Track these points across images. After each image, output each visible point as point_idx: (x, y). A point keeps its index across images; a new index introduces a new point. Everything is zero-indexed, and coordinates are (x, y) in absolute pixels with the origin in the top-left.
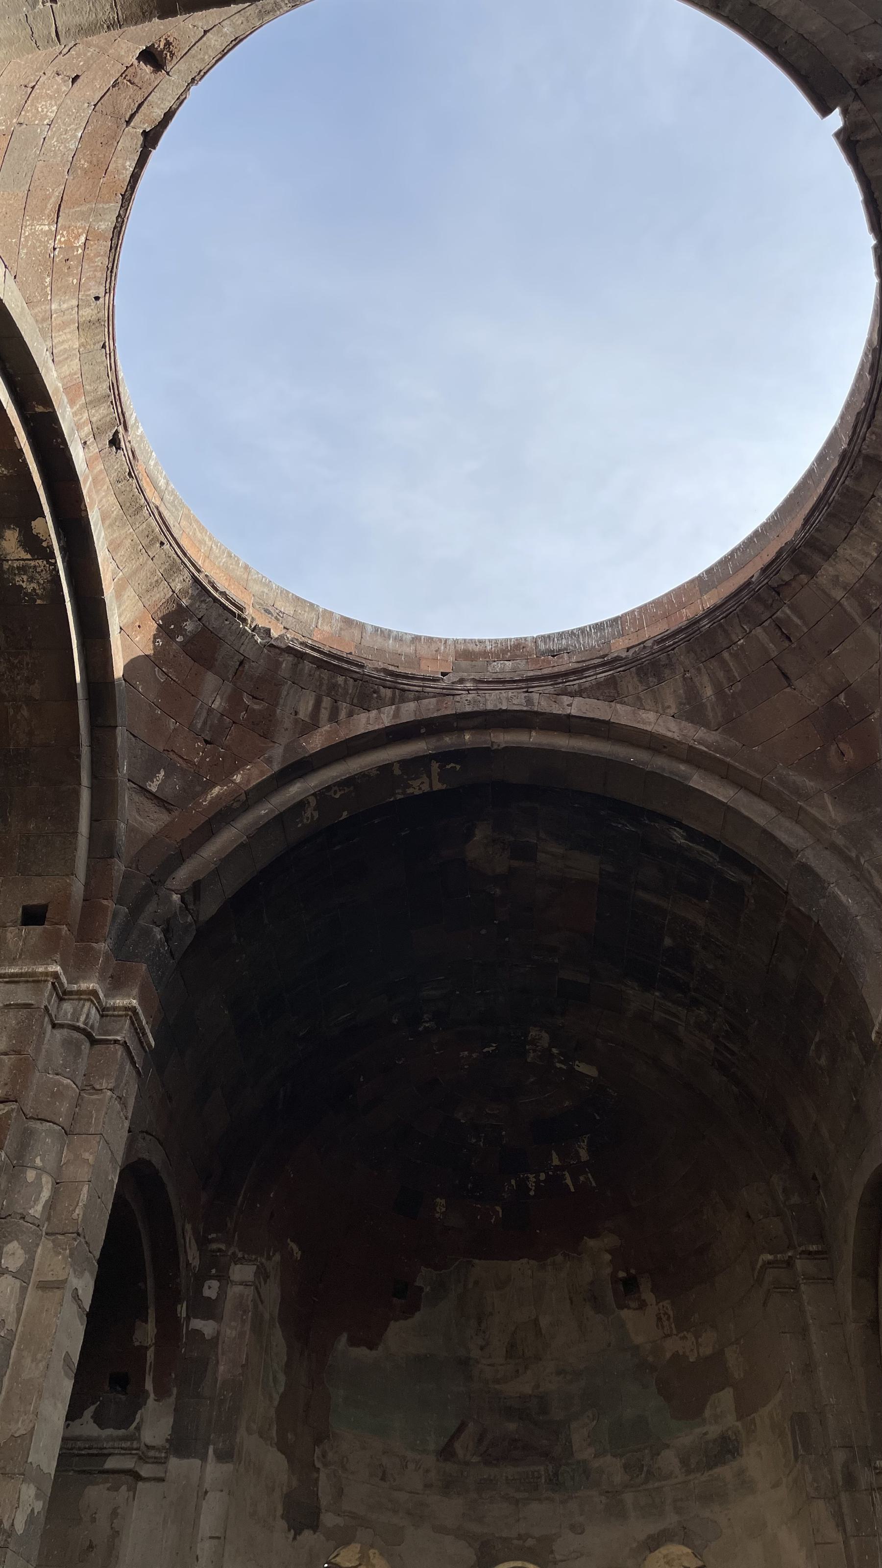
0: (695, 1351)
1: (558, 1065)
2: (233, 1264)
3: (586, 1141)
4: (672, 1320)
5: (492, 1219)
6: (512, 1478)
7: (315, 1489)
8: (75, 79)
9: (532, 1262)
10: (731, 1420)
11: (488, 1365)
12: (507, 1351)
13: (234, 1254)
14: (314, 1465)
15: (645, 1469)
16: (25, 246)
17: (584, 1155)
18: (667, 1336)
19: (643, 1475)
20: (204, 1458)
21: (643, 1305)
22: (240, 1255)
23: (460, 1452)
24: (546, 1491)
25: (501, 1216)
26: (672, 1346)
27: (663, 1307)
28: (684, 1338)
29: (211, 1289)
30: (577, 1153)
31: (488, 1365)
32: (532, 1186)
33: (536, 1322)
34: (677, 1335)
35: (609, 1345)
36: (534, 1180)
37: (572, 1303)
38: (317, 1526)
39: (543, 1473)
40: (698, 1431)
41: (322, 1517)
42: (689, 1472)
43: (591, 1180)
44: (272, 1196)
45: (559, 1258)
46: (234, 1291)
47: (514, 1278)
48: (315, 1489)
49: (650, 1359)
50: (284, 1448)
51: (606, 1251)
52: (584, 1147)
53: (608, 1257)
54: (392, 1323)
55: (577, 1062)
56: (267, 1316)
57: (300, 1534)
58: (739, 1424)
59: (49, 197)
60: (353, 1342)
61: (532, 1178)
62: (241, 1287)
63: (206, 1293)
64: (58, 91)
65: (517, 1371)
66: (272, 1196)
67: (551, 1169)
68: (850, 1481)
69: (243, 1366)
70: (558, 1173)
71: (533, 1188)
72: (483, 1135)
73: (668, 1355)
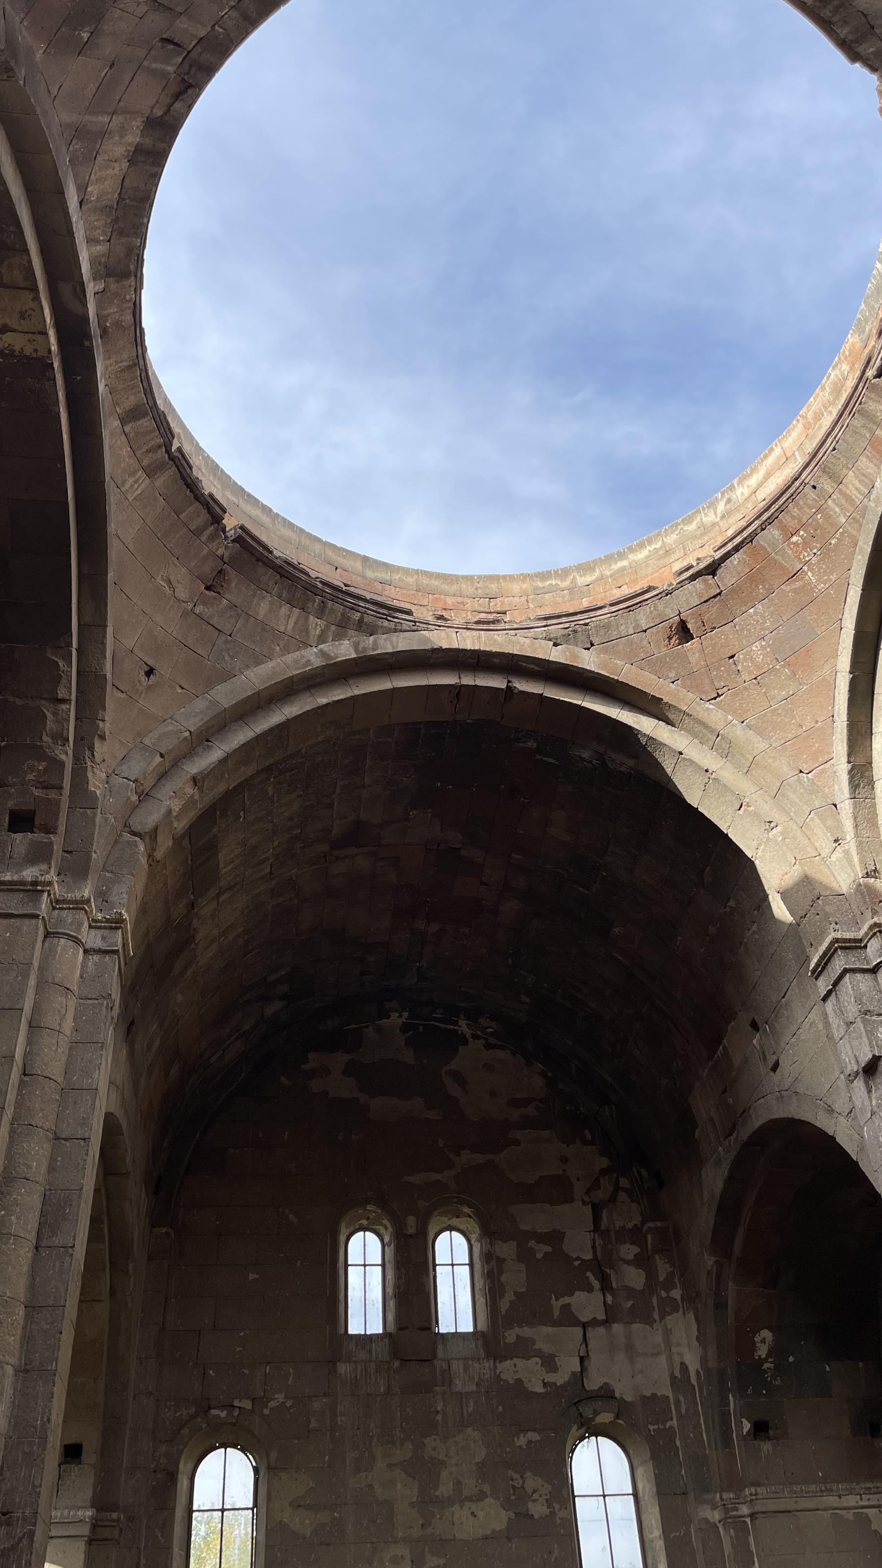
8: (733, 657)
16: (830, 580)
59: (795, 591)
64: (745, 660)
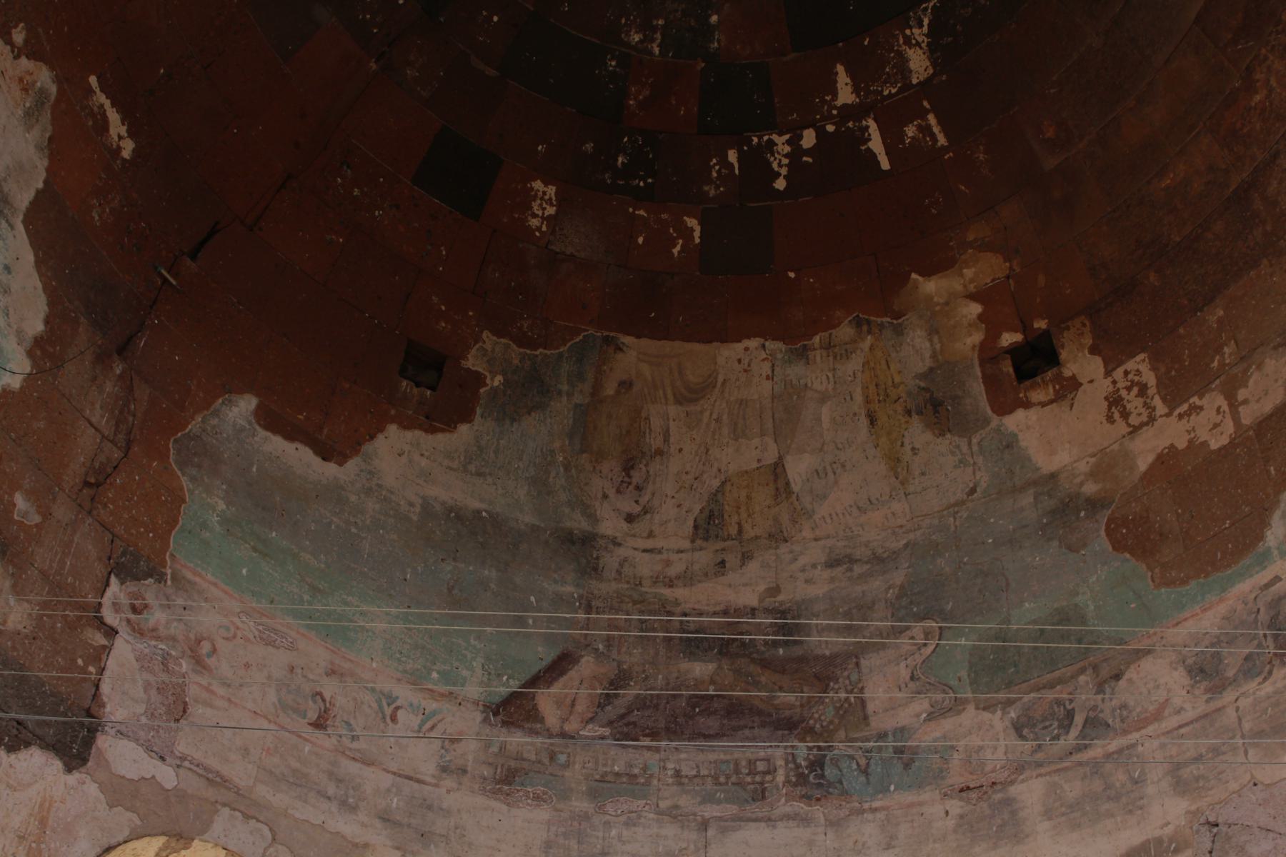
3: (926, 22)
5: (675, 246)
6: (694, 773)
9: (770, 345)
11: (645, 551)
12: (696, 527)
15: (1079, 719)
17: (919, 64)
18: (1135, 430)
21: (1070, 387)
23: (551, 715)
24: (786, 801)
25: (697, 240)
27: (1126, 373)
30: (903, 60)
31: (645, 551)
32: (780, 166)
33: (777, 469)
34: (1168, 415)
36: (787, 149)
37: (872, 420)
38: (84, 761)
39: (780, 763)
40: (1245, 587)
42: (1217, 689)
43: (936, 130)
45: (845, 331)
47: (725, 381)
48: (91, 669)
51: (973, 297)
52: (920, 40)
53: (975, 309)
54: (392, 429)
60: (270, 419)
61: (781, 141)
65: (722, 563)
67: (834, 116)
70: (850, 124)
71: (784, 171)
72: (661, 22)
73: (1143, 465)
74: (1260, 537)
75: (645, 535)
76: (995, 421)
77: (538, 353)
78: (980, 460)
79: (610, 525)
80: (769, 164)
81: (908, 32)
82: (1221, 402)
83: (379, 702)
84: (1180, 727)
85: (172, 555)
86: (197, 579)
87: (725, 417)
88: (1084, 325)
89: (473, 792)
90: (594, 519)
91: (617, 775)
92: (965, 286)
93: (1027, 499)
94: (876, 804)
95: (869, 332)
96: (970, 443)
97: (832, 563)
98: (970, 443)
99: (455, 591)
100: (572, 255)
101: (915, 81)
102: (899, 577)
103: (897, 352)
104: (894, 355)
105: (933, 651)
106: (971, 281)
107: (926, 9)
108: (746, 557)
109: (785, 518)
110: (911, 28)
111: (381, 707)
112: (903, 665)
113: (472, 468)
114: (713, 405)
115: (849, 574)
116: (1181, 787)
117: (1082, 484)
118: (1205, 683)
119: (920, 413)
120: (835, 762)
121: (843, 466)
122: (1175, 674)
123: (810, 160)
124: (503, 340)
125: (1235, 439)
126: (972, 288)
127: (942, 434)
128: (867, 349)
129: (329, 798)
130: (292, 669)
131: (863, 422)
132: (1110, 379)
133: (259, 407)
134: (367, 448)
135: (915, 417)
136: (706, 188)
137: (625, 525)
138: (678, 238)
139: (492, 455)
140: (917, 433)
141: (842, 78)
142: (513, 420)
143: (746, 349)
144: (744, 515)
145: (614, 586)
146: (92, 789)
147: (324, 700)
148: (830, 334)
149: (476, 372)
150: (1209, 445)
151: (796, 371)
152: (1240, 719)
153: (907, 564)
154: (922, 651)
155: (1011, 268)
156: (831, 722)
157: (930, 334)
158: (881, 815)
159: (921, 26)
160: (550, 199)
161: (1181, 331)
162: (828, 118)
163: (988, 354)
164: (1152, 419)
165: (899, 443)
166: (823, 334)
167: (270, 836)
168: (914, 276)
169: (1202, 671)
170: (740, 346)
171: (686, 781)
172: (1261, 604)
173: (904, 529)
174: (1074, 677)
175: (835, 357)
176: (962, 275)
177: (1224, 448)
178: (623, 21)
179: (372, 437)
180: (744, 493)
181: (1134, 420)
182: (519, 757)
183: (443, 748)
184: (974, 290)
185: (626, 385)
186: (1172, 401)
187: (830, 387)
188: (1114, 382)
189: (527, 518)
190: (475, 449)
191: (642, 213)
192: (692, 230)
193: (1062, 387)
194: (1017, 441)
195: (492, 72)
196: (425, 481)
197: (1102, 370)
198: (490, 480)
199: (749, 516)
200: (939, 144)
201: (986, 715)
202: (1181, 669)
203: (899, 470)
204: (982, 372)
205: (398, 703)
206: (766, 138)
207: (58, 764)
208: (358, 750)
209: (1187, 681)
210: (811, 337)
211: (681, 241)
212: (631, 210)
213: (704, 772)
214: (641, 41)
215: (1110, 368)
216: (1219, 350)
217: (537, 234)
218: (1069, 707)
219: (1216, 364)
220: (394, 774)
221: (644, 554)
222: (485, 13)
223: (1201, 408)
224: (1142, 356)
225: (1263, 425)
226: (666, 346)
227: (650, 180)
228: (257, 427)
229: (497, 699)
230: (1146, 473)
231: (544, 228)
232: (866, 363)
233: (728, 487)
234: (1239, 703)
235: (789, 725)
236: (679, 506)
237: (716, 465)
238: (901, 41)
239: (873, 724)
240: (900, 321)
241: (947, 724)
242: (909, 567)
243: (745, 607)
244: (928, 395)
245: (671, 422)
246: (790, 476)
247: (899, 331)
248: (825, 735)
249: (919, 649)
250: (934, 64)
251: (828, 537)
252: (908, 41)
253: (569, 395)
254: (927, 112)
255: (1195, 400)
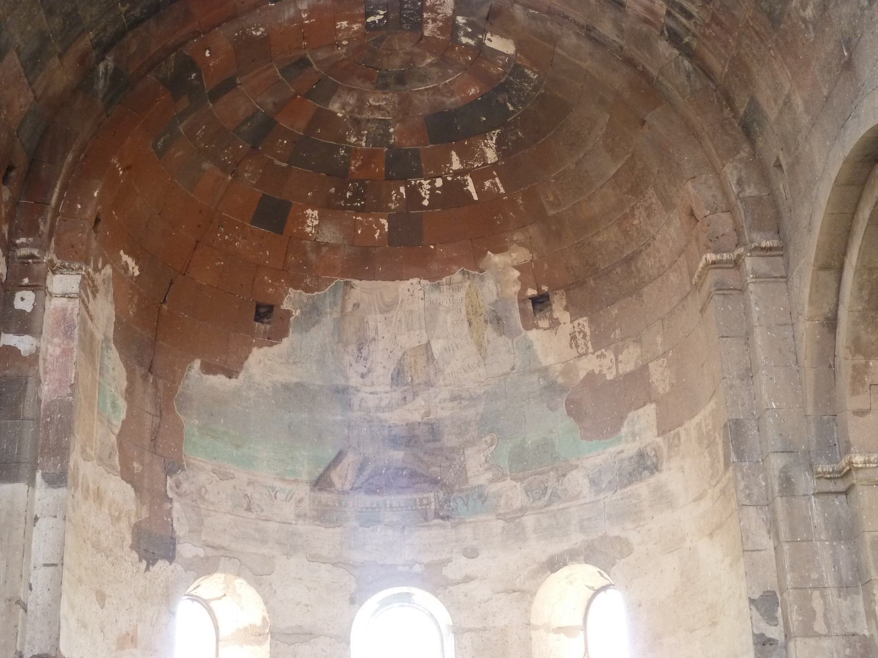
0: (614, 368)
1: (464, 40)
2: (50, 273)
4: (588, 338)
7: (169, 520)
9: (423, 282)
10: (650, 437)
12: (392, 379)
13: (51, 261)
14: (167, 496)
15: (549, 491)
17: (491, 156)
18: (580, 356)
19: (547, 497)
20: (32, 483)
21: (555, 324)
22: (58, 262)
25: (387, 230)
26: (588, 365)
27: (579, 324)
28: (602, 356)
29: (24, 301)
31: (371, 393)
32: (425, 194)
33: (428, 346)
34: (593, 354)
35: (513, 369)
36: (429, 187)
37: (470, 324)
38: (174, 557)
39: (433, 500)
40: (612, 449)
41: (179, 547)
42: (598, 493)
43: (500, 185)
44: (95, 195)
45: (457, 277)
46: (54, 304)
48: (169, 520)
49: (560, 380)
50: (127, 475)
51: (517, 268)
53: (516, 274)
54: (255, 350)
55: (489, 35)
56: (99, 336)
57: (153, 564)
58: (660, 440)
60: (209, 369)
61: (426, 184)
62: (64, 300)
63: (18, 304)
65: (405, 398)
66: (95, 195)
68: (787, 485)
69: (71, 386)
70: (459, 178)
71: (427, 197)
72: (366, 132)
73: (582, 375)
74: (620, 430)
75: (370, 384)
76: (524, 332)
77: (314, 294)
78: (517, 352)
79: (355, 380)
80: (420, 193)
81: (486, 141)
82: (613, 357)
83: (269, 491)
84: (585, 504)
85: (185, 455)
86: (195, 462)
87: (403, 319)
88: (563, 294)
89: (310, 524)
90: (347, 378)
91: (367, 508)
92: (512, 261)
93: (535, 378)
94: (472, 520)
95: (469, 278)
96: (513, 341)
97: (453, 399)
98: (513, 341)
99: (292, 428)
100: (327, 243)
101: (489, 162)
102: (481, 409)
103: (481, 290)
104: (480, 291)
105: (495, 449)
106: (515, 259)
107: (494, 133)
108: (415, 395)
109: (432, 372)
110: (487, 140)
111: (269, 493)
112: (482, 454)
113: (291, 361)
114: (397, 314)
115: (460, 405)
116: (583, 529)
117: (558, 376)
118: (595, 488)
119: (491, 322)
120: (454, 499)
121: (457, 347)
122: (585, 481)
123: (440, 192)
124: (298, 291)
125: (616, 378)
126: (515, 263)
127: (501, 335)
128: (467, 287)
129: (256, 540)
130: (234, 487)
131: (466, 324)
132: (572, 325)
133: (202, 364)
134: (246, 364)
135: (489, 325)
136: (390, 205)
137: (361, 380)
138: (377, 229)
139: (299, 352)
140: (489, 333)
141: (455, 157)
142: (307, 331)
143: (412, 284)
144: (413, 372)
145: (359, 414)
146: (179, 568)
147: (248, 497)
148: (451, 278)
149: (288, 310)
150: (606, 377)
151: (435, 296)
152: (605, 507)
153: (484, 403)
154: (490, 448)
155: (533, 257)
156: (453, 481)
157: (496, 283)
158: (472, 525)
159: (492, 139)
160: (315, 217)
161: (601, 312)
162: (449, 173)
163: (522, 300)
164: (586, 354)
165: (482, 337)
166: (446, 277)
167: (239, 563)
168: (489, 253)
169: (594, 482)
170: (408, 282)
171: (394, 509)
172: (616, 460)
173: (484, 384)
174: (549, 472)
175: (453, 289)
176: (511, 256)
177: (611, 380)
178: (347, 133)
179: (247, 358)
180: (413, 359)
181: (581, 351)
182: (327, 505)
183: (296, 506)
184: (516, 264)
185: (356, 305)
186: (597, 346)
187: (451, 305)
188: (574, 327)
189: (319, 382)
190: (291, 350)
191: (359, 218)
192: (384, 225)
193: (553, 322)
194: (533, 345)
195: (285, 165)
196: (272, 373)
197: (569, 319)
198: (299, 365)
199: (416, 372)
200: (501, 192)
201: (514, 483)
202: (587, 479)
203: (482, 351)
204: (519, 306)
205: (276, 490)
206: (418, 181)
207: (167, 563)
208: (264, 516)
209: (588, 485)
210: (441, 278)
211: (379, 231)
212: (354, 217)
213: (402, 505)
214: (356, 141)
215: (573, 319)
216: (614, 330)
217: (310, 235)
218: (546, 485)
219: (613, 336)
220: (279, 522)
221: (371, 395)
222: (280, 141)
223: (605, 356)
224: (585, 318)
225: (627, 376)
226: (373, 283)
227: (363, 203)
228: (203, 375)
229: (315, 479)
230: (582, 380)
231: (313, 232)
232: (467, 294)
233: (406, 357)
234: (606, 500)
235: (434, 482)
236: (384, 367)
237: (399, 344)
238: (483, 145)
239: (470, 482)
240: (483, 274)
241: (500, 485)
242: (485, 405)
243: (416, 422)
244: (495, 314)
245: (378, 323)
246: (433, 351)
247: (482, 279)
248: (451, 486)
249: (489, 447)
250: (498, 156)
251: (450, 385)
252: (486, 145)
253: (331, 314)
254: (495, 177)
255: (603, 350)
